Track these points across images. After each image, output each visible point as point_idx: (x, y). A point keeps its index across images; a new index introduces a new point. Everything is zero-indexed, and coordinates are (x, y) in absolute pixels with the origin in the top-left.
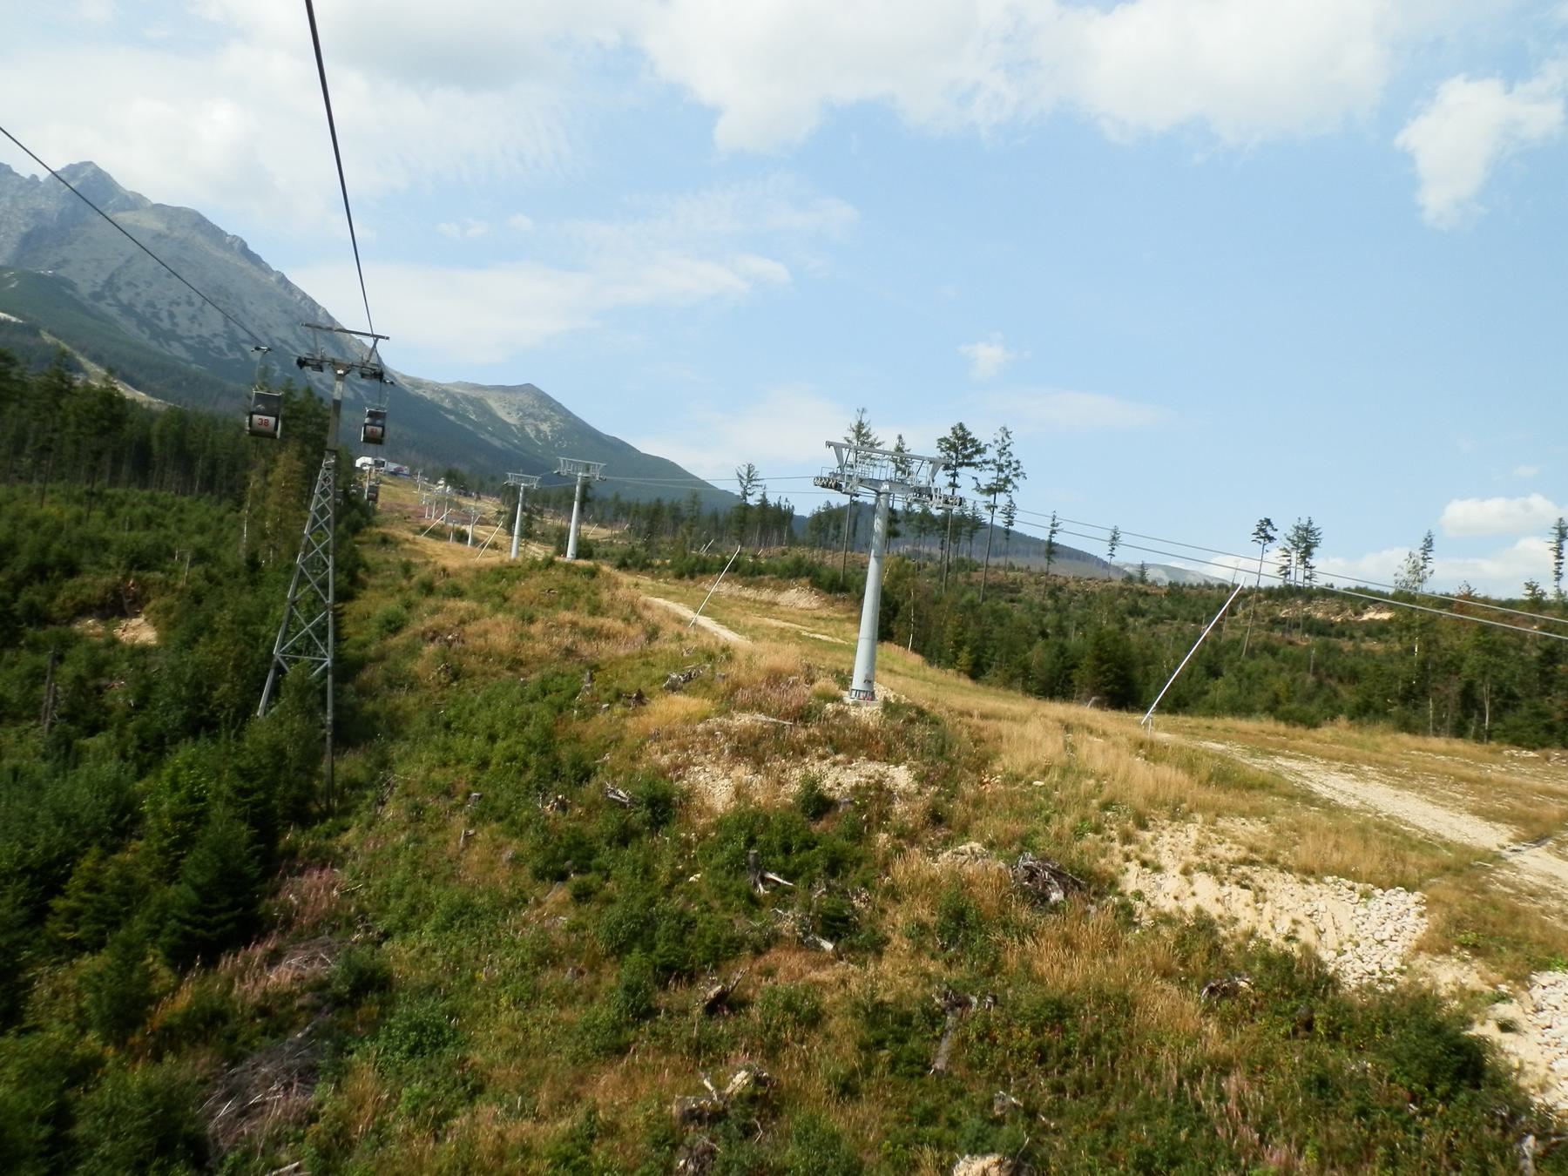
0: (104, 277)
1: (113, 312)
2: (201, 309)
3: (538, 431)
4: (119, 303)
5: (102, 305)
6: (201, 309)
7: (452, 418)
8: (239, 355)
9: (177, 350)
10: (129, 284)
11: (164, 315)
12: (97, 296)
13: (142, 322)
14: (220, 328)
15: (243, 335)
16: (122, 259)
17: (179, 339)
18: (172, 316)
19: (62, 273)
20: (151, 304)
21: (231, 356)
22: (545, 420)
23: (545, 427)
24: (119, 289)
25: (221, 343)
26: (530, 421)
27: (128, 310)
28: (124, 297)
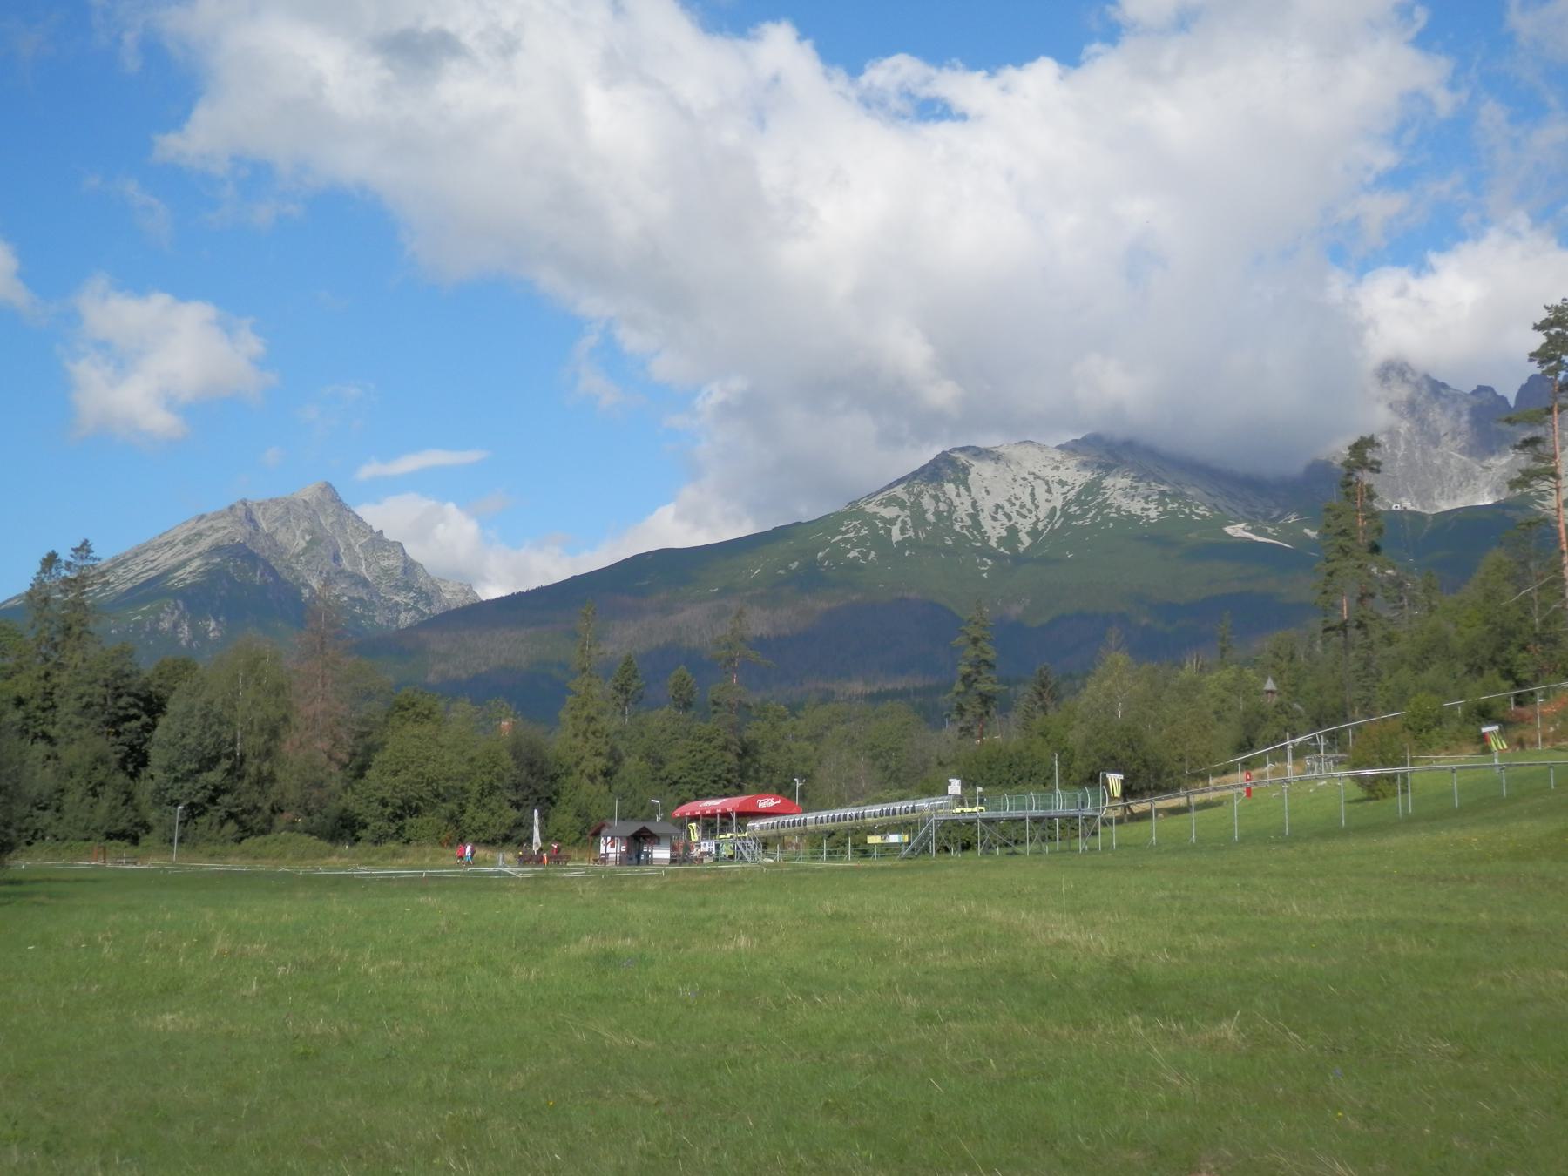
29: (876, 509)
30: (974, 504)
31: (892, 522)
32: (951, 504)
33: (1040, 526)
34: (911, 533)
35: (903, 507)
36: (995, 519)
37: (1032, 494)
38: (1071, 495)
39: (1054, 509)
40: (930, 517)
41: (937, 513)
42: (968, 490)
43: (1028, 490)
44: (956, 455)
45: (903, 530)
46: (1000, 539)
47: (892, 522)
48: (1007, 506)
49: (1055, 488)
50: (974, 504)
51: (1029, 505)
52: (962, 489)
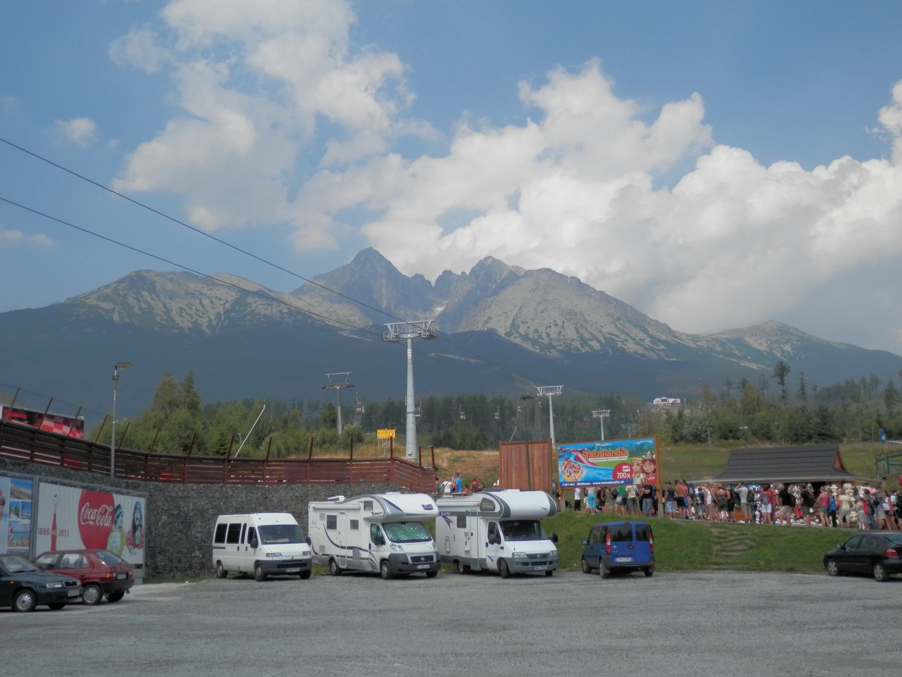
0: (510, 322)
1: (518, 341)
2: (563, 327)
3: (783, 351)
4: (521, 335)
5: (512, 339)
6: (563, 327)
7: (721, 356)
8: (588, 348)
9: (554, 353)
10: (523, 322)
11: (544, 335)
12: (509, 334)
13: (534, 342)
14: (575, 336)
15: (587, 336)
16: (516, 309)
17: (555, 347)
18: (548, 334)
19: (489, 325)
20: (536, 331)
21: (584, 351)
22: (786, 343)
23: (787, 348)
24: (519, 327)
25: (577, 344)
26: (776, 345)
27: (525, 338)
28: (522, 331)
29: (95, 303)
30: (164, 305)
31: (112, 311)
32: (148, 304)
33: (214, 323)
34: (127, 320)
35: (115, 303)
36: (182, 317)
37: (201, 303)
38: (228, 306)
39: (219, 314)
40: (136, 309)
41: (140, 308)
42: (158, 296)
43: (198, 301)
44: (144, 274)
45: (121, 316)
46: (190, 329)
47: (112, 311)
48: (187, 309)
49: (214, 300)
50: (164, 305)
51: (201, 309)
52: (154, 296)
